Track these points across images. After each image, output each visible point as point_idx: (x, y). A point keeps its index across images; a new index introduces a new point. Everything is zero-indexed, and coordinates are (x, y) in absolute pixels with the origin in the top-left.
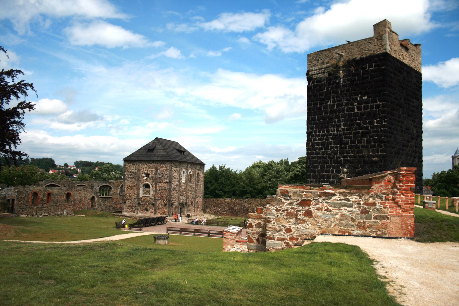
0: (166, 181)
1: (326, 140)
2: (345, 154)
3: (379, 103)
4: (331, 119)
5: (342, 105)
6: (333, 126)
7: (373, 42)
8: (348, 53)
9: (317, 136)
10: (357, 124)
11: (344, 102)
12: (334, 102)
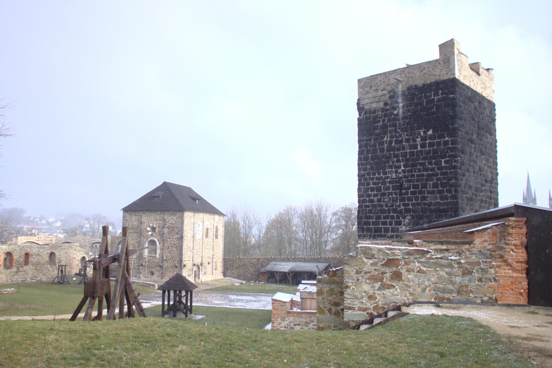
0: (176, 236)
2: (406, 202)
3: (447, 139)
4: (389, 158)
5: (402, 141)
6: (391, 167)
7: (439, 66)
8: (408, 78)
9: (370, 179)
10: (421, 164)
12: (391, 137)
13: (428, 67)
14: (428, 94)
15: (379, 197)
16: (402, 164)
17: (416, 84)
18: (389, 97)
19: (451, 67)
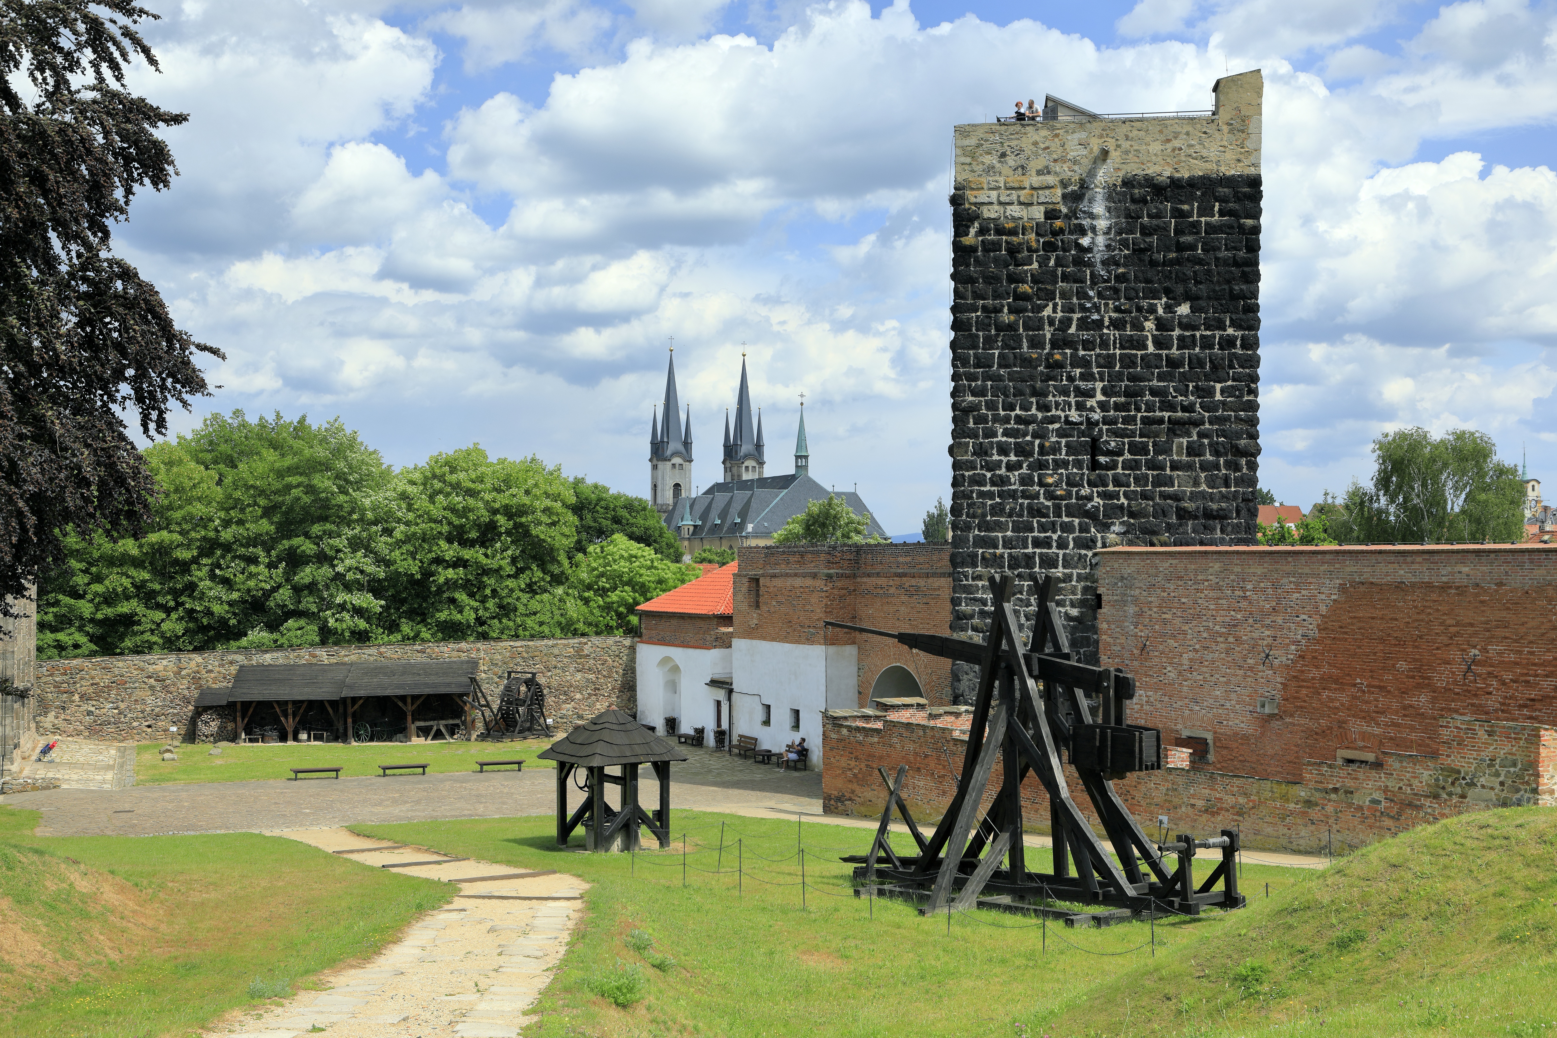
1: (1035, 436)
2: (1111, 488)
3: (1230, 331)
5: (1099, 324)
6: (1065, 392)
7: (1217, 135)
8: (1127, 152)
9: (996, 419)
10: (1154, 392)
13: (1188, 134)
14: (1186, 207)
15: (1024, 470)
16: (1099, 385)
17: (1149, 172)
18: (1064, 196)
19: (1250, 145)
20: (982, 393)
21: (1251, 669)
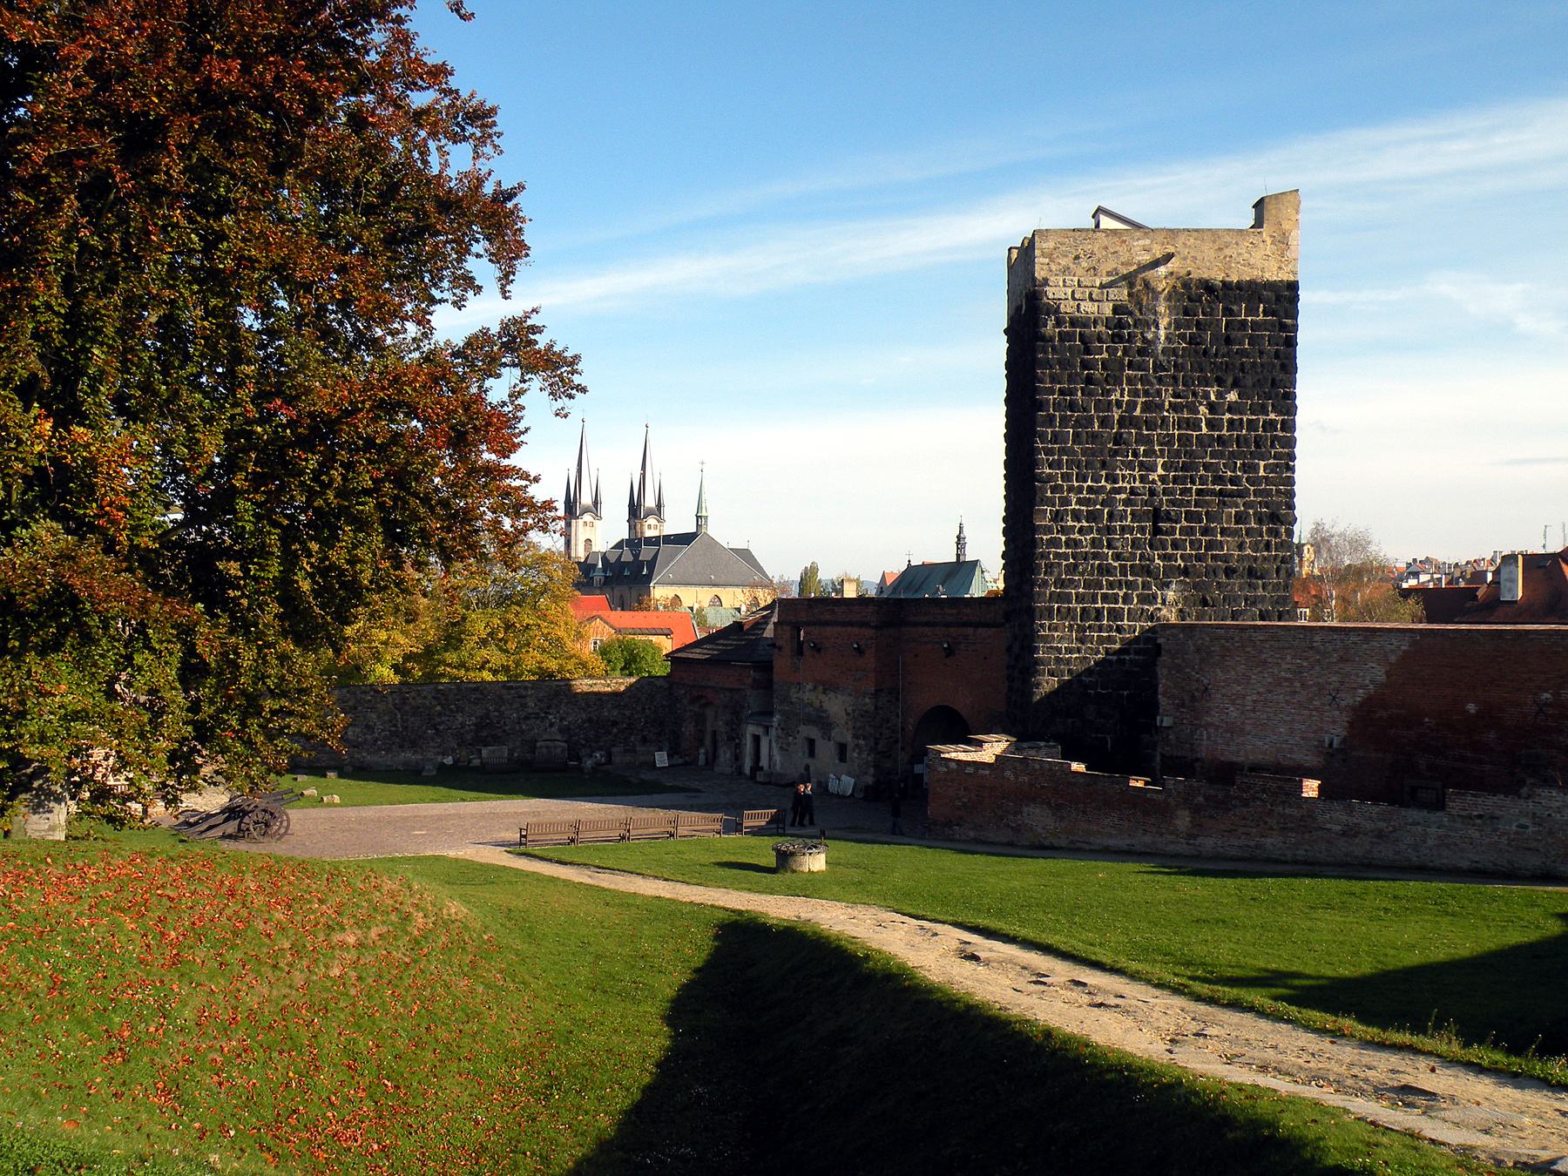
2: (1169, 551)
3: (1272, 416)
5: (1160, 407)
9: (1070, 489)
10: (1206, 467)
11: (1168, 400)
12: (1135, 393)
16: (1160, 461)
20: (1058, 464)
21: (1316, 709)
